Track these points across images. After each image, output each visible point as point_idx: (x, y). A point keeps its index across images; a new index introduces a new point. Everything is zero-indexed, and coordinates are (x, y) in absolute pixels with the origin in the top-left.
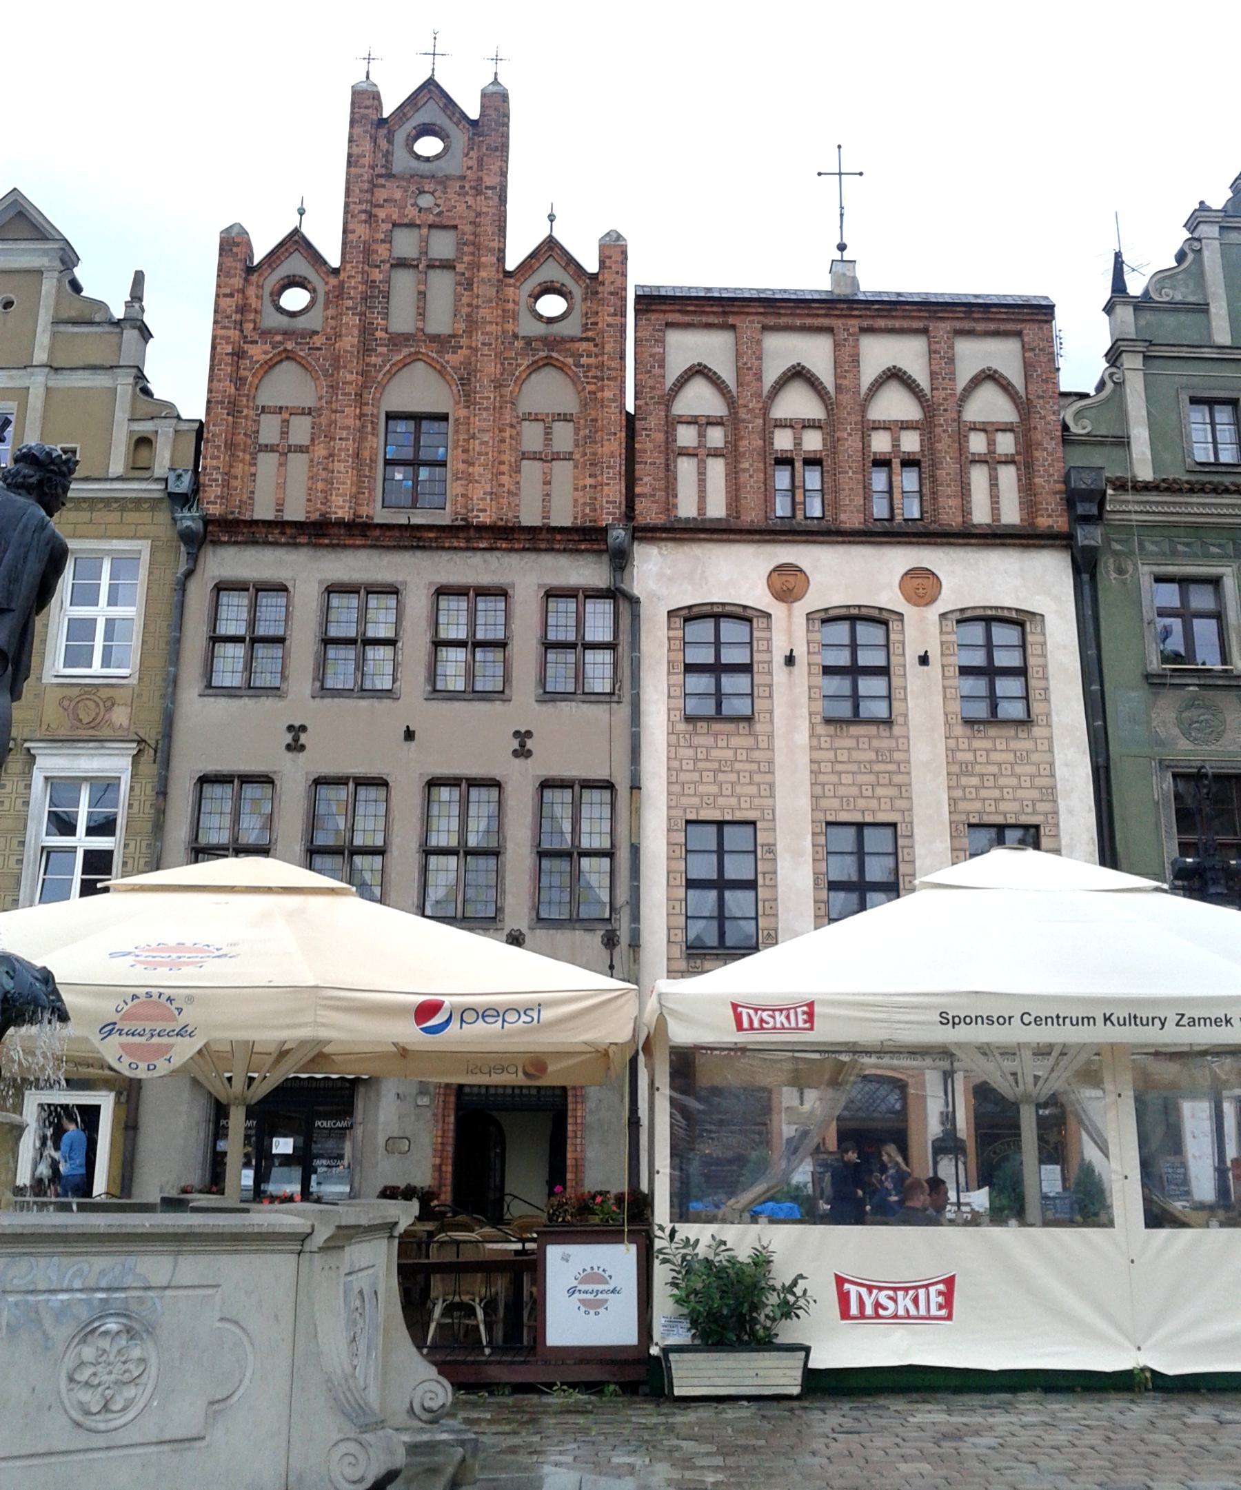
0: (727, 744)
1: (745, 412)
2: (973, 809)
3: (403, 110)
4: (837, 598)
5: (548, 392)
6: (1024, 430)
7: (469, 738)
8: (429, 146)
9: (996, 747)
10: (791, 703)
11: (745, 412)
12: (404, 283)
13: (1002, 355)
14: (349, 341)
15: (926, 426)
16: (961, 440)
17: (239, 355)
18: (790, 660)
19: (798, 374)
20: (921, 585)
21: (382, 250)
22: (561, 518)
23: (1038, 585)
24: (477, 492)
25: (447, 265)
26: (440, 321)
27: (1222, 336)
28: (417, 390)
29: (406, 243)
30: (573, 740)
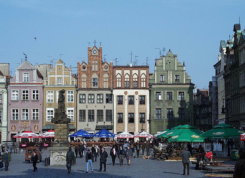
0: (121, 106)
1: (123, 77)
2: (140, 112)
3: (92, 49)
4: (130, 94)
5: (106, 75)
6: (146, 79)
7: (100, 107)
8: (95, 52)
9: (142, 106)
10: (126, 103)
11: (123, 77)
12: (93, 65)
13: (145, 72)
14: (89, 72)
15: (138, 78)
16: (141, 80)
17: (80, 73)
18: (126, 100)
19: (127, 74)
20: (137, 93)
21: (91, 63)
22: (107, 87)
23: (146, 93)
24: (100, 85)
25: (97, 64)
26: (97, 70)
27: (164, 69)
28: (95, 76)
29: (93, 62)
30: (109, 106)
